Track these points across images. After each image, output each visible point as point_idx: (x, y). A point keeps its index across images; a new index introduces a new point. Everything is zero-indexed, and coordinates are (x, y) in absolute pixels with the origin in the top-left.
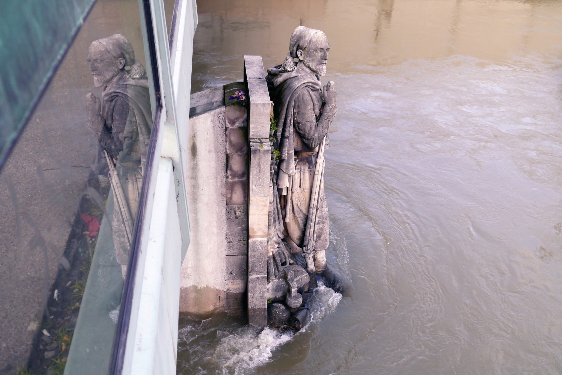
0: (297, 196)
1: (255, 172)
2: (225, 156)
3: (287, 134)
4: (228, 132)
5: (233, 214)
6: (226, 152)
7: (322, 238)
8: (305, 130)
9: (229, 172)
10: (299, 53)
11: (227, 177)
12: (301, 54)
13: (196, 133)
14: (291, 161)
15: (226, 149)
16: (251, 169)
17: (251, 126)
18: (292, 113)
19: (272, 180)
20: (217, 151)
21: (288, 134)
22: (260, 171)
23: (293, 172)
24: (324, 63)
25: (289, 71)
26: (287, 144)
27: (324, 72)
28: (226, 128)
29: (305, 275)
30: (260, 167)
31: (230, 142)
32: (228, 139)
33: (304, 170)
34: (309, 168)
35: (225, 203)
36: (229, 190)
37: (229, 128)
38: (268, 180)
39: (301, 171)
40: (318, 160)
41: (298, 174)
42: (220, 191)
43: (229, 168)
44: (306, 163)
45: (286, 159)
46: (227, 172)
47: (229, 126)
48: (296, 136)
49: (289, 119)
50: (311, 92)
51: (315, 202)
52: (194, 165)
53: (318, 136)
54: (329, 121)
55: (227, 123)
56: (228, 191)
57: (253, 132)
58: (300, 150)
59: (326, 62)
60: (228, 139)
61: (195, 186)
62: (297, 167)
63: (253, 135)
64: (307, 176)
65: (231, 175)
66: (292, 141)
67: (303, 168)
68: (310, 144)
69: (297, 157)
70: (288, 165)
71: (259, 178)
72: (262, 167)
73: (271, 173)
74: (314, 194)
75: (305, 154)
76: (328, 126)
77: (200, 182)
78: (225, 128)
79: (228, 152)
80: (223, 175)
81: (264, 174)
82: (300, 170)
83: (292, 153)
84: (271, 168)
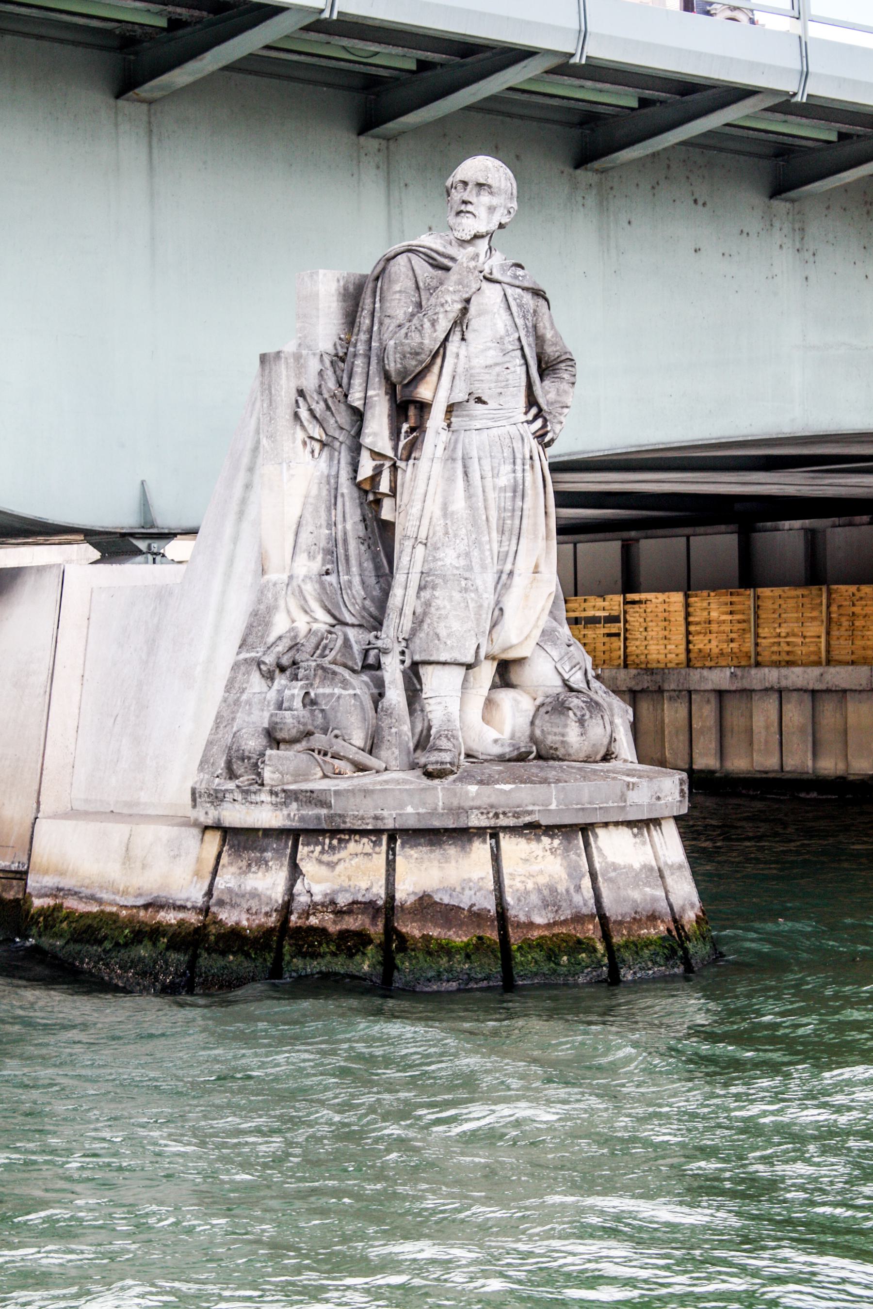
7: (425, 626)
23: (374, 443)
24: (461, 212)
29: (352, 692)
30: (270, 393)
45: (358, 404)
59: (469, 208)
71: (271, 419)
73: (296, 416)
84: (297, 401)
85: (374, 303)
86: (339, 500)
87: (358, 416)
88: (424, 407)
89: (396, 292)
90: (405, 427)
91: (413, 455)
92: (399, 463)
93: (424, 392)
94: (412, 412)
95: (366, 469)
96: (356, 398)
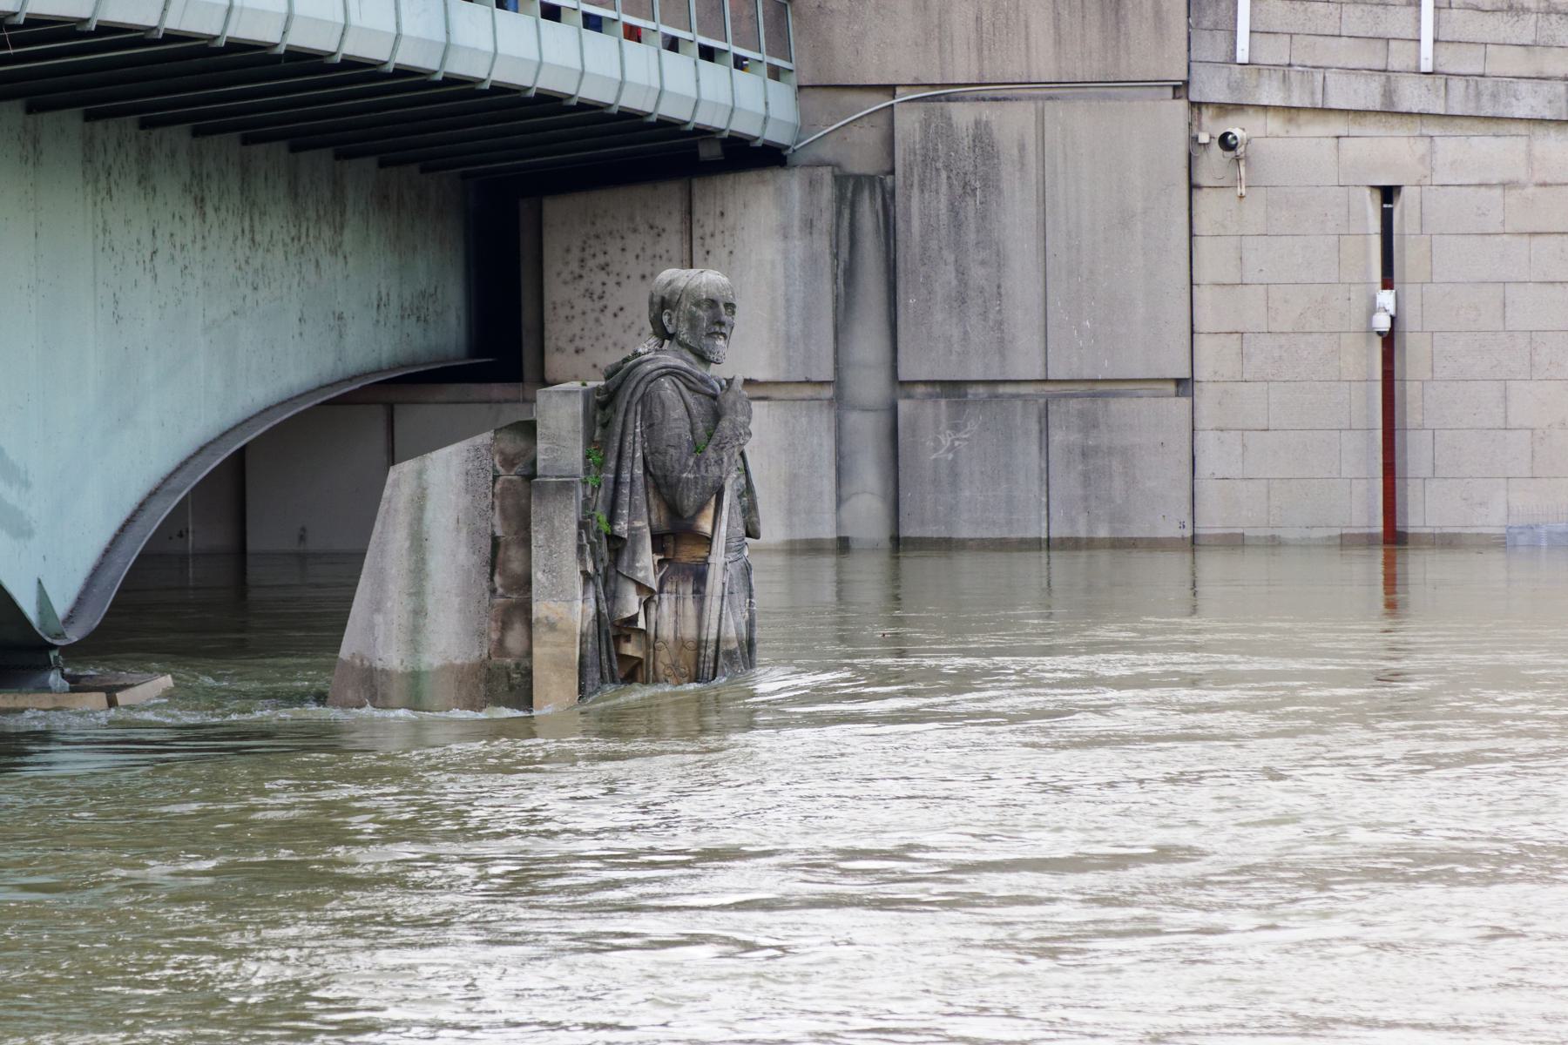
0: (667, 661)
1: (541, 537)
2: (490, 541)
3: (626, 476)
4: (498, 486)
5: (505, 679)
6: (493, 533)
8: (664, 464)
9: (497, 579)
10: (665, 318)
11: (493, 591)
12: (670, 320)
13: (425, 489)
14: (640, 548)
15: (492, 526)
16: (534, 528)
17: (541, 445)
18: (638, 430)
19: (591, 583)
20: (474, 532)
21: (628, 475)
22: (552, 536)
23: (646, 578)
24: (716, 333)
25: (640, 354)
26: (627, 499)
27: (721, 354)
28: (495, 479)
31: (503, 510)
32: (497, 503)
33: (684, 594)
34: (694, 592)
35: (486, 652)
36: (496, 621)
37: (501, 478)
38: (570, 559)
39: (677, 598)
40: (711, 560)
41: (670, 605)
42: (475, 624)
43: (497, 571)
44: (688, 580)
45: (626, 536)
46: (492, 579)
47: (502, 470)
48: (654, 497)
49: (630, 438)
50: (681, 386)
51: (707, 665)
52: (417, 562)
53: (695, 478)
54: (723, 448)
55: (499, 467)
56: (493, 624)
57: (544, 460)
58: (665, 529)
59: (724, 330)
60: (497, 503)
61: (419, 612)
62: (668, 587)
63: (545, 467)
64: (690, 607)
65: (502, 586)
66: (640, 498)
67: (681, 590)
68: (678, 497)
69: (661, 557)
70: (633, 560)
72: (557, 524)
73: (581, 549)
74: (704, 644)
75: (688, 553)
76: (722, 460)
77: (430, 602)
78: (491, 478)
79: (499, 532)
80: (484, 587)
81: (562, 541)
82: (674, 595)
83: (639, 528)
84: (580, 535)
85: (636, 427)
86: (603, 637)
87: (617, 545)
88: (708, 541)
89: (676, 420)
90: (658, 558)
91: (665, 589)
92: (656, 598)
93: (705, 525)
94: (670, 545)
95: (631, 604)
96: (622, 527)
